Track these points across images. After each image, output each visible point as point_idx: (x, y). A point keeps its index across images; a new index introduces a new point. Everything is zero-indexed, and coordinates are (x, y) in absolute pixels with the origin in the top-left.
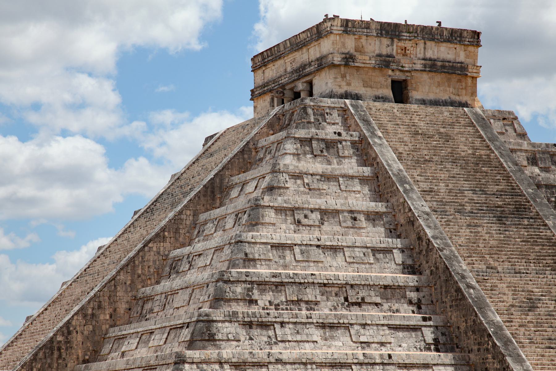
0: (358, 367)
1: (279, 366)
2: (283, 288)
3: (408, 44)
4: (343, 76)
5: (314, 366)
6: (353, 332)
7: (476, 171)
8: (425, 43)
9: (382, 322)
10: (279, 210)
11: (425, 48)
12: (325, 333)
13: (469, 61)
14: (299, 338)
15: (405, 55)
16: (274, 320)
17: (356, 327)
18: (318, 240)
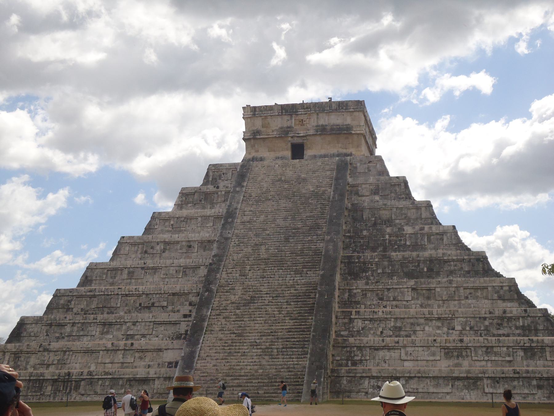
0: (105, 352)
1: (46, 354)
2: (95, 299)
3: (304, 117)
4: (253, 146)
5: (71, 353)
6: (124, 327)
7: (302, 204)
8: (318, 115)
9: (150, 320)
11: (317, 118)
12: (103, 330)
13: (354, 123)
14: (81, 333)
15: (303, 125)
16: (68, 322)
17: (128, 324)
18: (145, 264)
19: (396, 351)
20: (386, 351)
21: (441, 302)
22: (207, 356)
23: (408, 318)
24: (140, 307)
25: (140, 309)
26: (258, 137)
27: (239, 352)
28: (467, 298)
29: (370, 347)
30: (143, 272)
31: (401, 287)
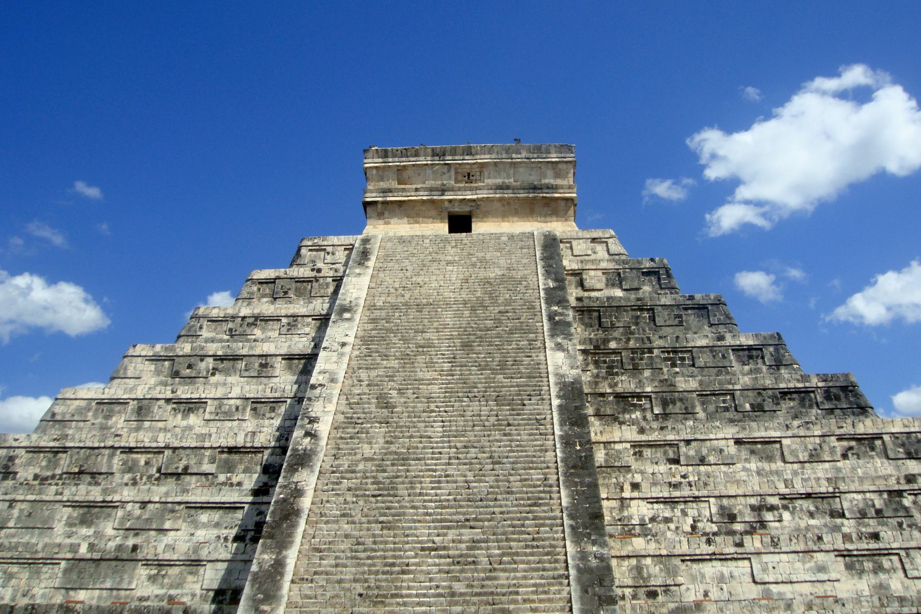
2: (64, 455)
9: (178, 499)
10: (156, 359)
17: (129, 507)
18: (173, 392)
19: (740, 563)
20: (717, 564)
21: (796, 466)
22: (316, 573)
23: (745, 496)
24: (157, 475)
25: (158, 479)
26: (388, 199)
27: (393, 565)
28: (845, 456)
29: (684, 558)
30: (169, 407)
31: (712, 436)
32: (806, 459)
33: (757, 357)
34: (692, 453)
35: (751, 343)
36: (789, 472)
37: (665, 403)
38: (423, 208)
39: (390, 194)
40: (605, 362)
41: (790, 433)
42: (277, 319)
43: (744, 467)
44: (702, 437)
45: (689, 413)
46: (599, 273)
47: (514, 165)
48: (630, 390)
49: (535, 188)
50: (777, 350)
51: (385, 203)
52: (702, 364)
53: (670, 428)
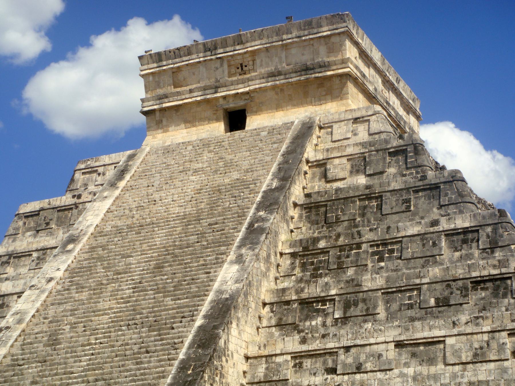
21: (457, 368)
31: (372, 341)
32: (469, 359)
33: (472, 241)
34: (350, 360)
35: (467, 225)
36: (447, 375)
37: (347, 306)
38: (199, 109)
39: (166, 100)
40: (312, 263)
41: (455, 331)
42: (27, 254)
43: (401, 372)
44: (362, 343)
45: (369, 315)
46: (344, 160)
47: (285, 47)
48: (315, 295)
49: (306, 69)
50: (495, 231)
51: (163, 110)
52: (409, 256)
53: (331, 335)
